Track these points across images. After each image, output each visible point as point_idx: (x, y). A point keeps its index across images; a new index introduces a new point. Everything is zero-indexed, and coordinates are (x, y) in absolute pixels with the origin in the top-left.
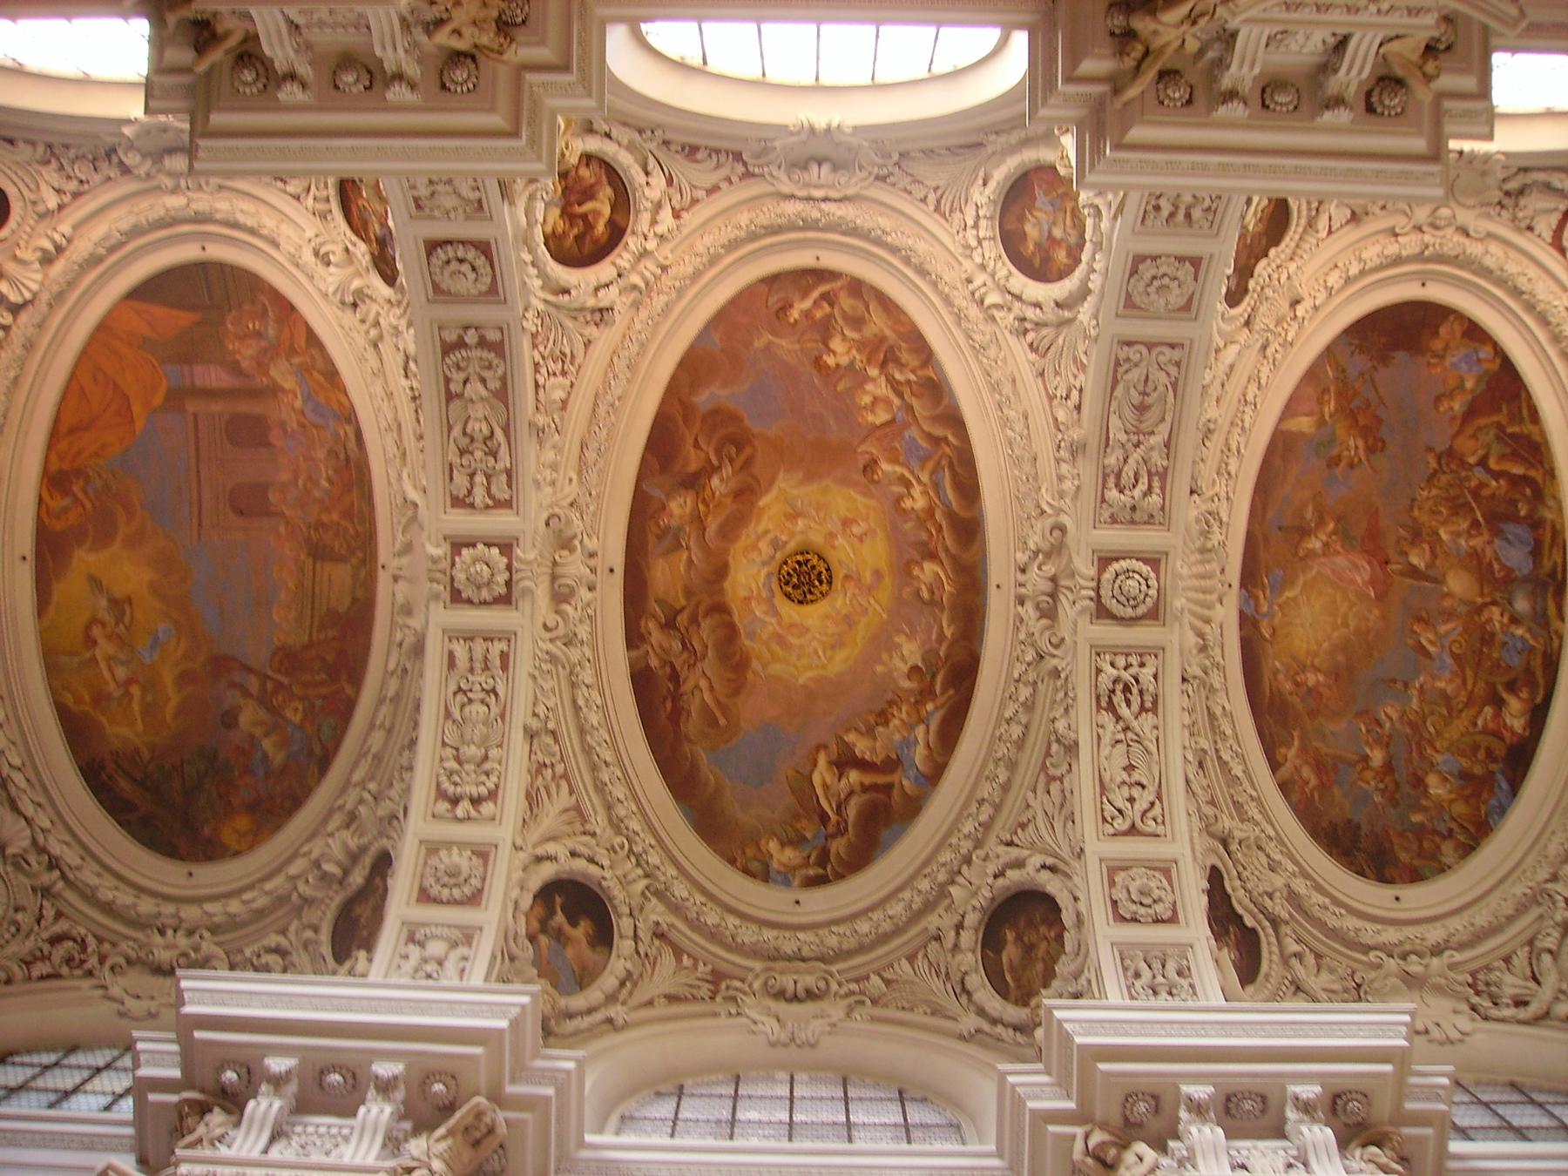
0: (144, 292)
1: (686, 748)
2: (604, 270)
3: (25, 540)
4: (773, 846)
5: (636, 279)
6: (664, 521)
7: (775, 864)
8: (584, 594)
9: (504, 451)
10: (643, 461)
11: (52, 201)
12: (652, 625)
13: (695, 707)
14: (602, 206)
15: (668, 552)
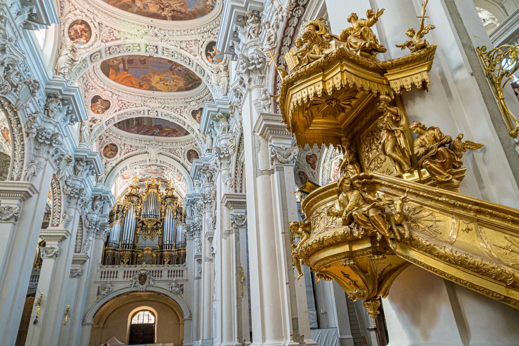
0: (107, 75)
1: (187, 12)
2: (91, 25)
3: (151, 92)
4: (207, 3)
5: (92, 17)
6: (142, 8)
7: (211, 4)
8: (156, 31)
9: (129, 45)
10: (129, 12)
11: (94, 90)
12: (163, 13)
13: (180, 8)
14: (78, 27)
15: (148, 7)
